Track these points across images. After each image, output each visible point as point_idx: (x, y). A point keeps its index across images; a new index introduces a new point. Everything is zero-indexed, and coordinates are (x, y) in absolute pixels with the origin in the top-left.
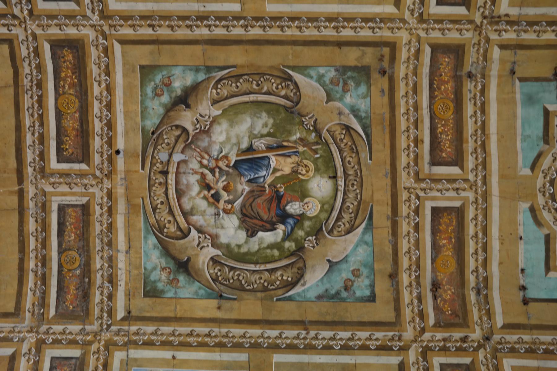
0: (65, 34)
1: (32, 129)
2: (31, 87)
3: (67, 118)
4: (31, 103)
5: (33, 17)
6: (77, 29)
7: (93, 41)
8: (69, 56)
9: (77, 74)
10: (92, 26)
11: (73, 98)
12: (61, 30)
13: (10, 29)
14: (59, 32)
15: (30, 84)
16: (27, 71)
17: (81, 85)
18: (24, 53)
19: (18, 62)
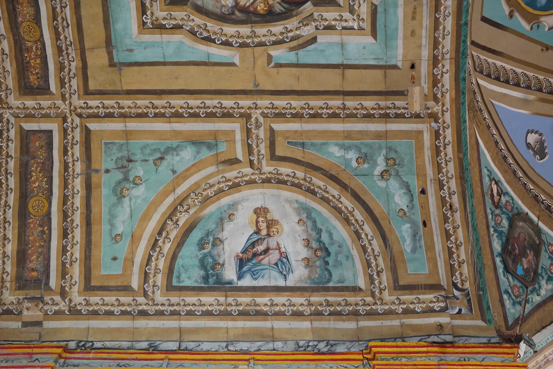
0: (36, 100)
1: (63, 5)
2: (67, 49)
3: (30, 16)
4: (65, 32)
5: (63, 115)
6: (25, 105)
7: (10, 94)
8: (33, 79)
9: (25, 61)
10: (11, 108)
11: (26, 38)
12: (39, 103)
13: (86, 105)
14: (41, 102)
15: (69, 51)
16: (73, 64)
17: (21, 50)
18: (74, 82)
19: (80, 73)
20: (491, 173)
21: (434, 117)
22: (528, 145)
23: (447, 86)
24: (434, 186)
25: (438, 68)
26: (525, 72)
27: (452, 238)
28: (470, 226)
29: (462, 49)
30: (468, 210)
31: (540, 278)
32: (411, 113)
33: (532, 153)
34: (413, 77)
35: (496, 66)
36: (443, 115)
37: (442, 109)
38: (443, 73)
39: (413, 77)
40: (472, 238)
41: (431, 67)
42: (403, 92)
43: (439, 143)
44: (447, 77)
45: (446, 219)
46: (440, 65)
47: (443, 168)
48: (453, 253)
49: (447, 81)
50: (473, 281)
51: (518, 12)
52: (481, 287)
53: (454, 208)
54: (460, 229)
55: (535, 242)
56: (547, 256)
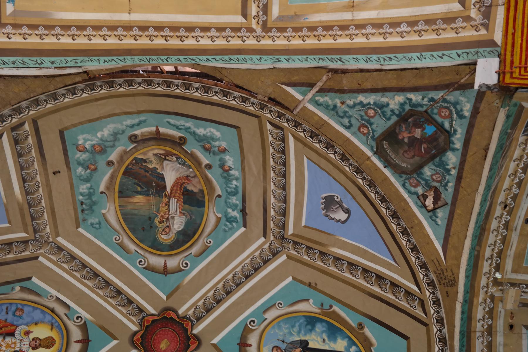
20: (431, 217)
21: (496, 282)
22: (347, 211)
23: (480, 308)
24: (513, 224)
25: (487, 325)
26: (340, 272)
27: (517, 180)
28: (492, 190)
29: (465, 339)
30: (488, 203)
31: (397, 112)
32: (520, 288)
33: (344, 204)
34: (512, 318)
35: (380, 287)
36: (487, 284)
37: (488, 289)
38: (484, 320)
39: (512, 318)
40: (496, 180)
41: (493, 325)
42: (523, 306)
43: (497, 260)
44: (479, 316)
45: (515, 197)
46: (486, 327)
47: (500, 240)
48: (522, 169)
49: (479, 312)
50: (514, 143)
51: (351, 326)
52: (506, 137)
53: (503, 206)
54: (504, 188)
55: (390, 144)
56: (374, 126)
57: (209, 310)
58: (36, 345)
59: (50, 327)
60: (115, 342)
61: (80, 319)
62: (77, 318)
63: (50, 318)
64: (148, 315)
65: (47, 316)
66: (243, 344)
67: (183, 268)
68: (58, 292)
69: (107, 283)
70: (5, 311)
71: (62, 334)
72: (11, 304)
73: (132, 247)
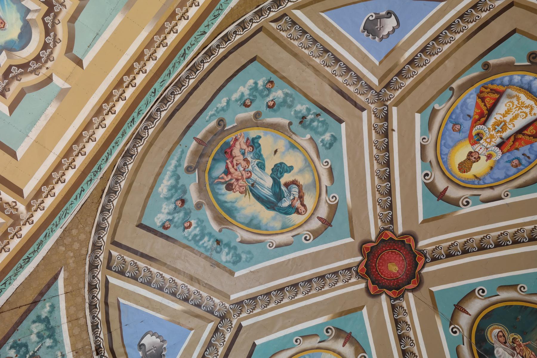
57: (397, 323)
58: (472, 156)
59: (478, 176)
60: (421, 219)
61: (466, 204)
62: (468, 203)
63: (486, 181)
64: (426, 263)
65: (492, 180)
66: (349, 338)
67: (452, 326)
68: (507, 204)
69: (482, 249)
70: (528, 155)
71: (463, 182)
72: (530, 163)
73: (504, 295)
